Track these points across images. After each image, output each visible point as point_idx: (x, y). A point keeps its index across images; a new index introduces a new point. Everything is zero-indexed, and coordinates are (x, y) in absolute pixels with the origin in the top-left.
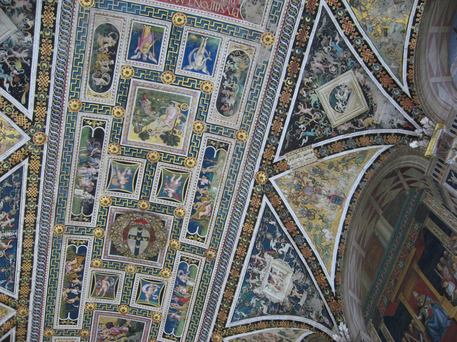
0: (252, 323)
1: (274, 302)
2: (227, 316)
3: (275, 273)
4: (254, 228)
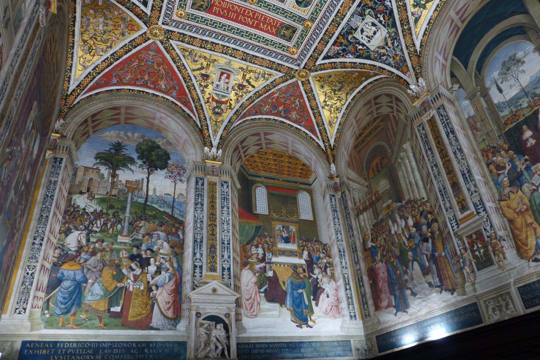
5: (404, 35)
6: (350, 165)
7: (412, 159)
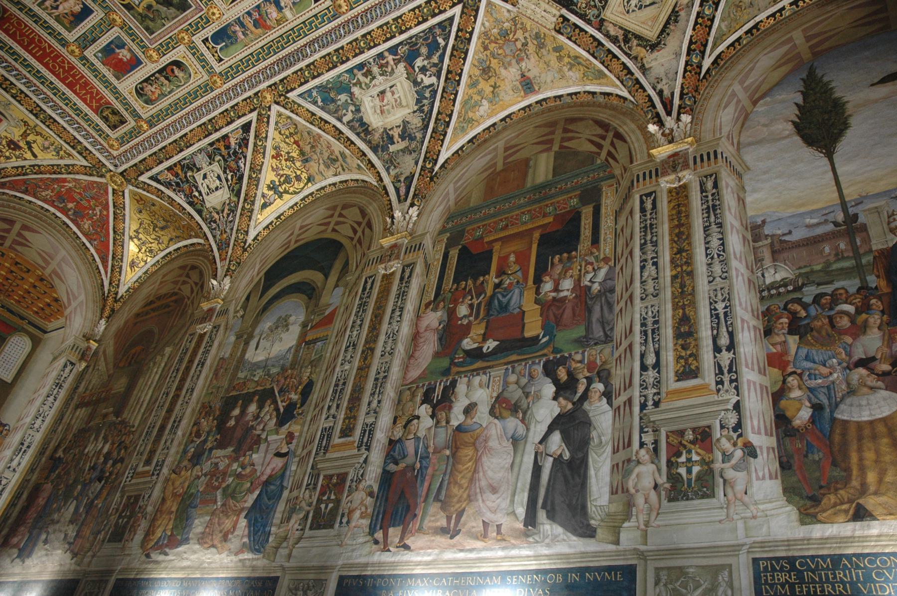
0: (320, 118)
1: (365, 120)
2: (299, 86)
3: (393, 93)
4: (416, 25)
5: (241, 214)
6: (119, 335)
7: (160, 372)
